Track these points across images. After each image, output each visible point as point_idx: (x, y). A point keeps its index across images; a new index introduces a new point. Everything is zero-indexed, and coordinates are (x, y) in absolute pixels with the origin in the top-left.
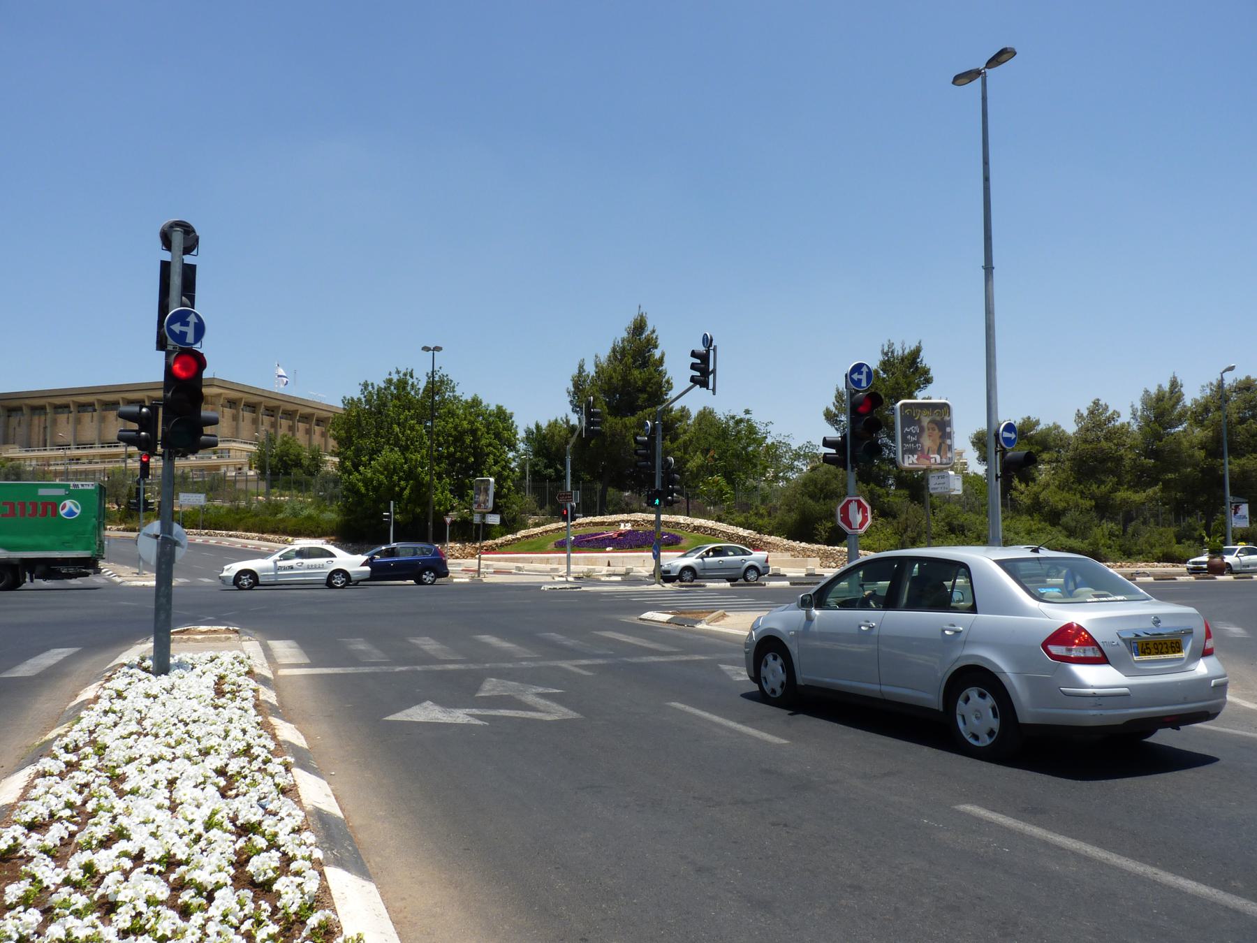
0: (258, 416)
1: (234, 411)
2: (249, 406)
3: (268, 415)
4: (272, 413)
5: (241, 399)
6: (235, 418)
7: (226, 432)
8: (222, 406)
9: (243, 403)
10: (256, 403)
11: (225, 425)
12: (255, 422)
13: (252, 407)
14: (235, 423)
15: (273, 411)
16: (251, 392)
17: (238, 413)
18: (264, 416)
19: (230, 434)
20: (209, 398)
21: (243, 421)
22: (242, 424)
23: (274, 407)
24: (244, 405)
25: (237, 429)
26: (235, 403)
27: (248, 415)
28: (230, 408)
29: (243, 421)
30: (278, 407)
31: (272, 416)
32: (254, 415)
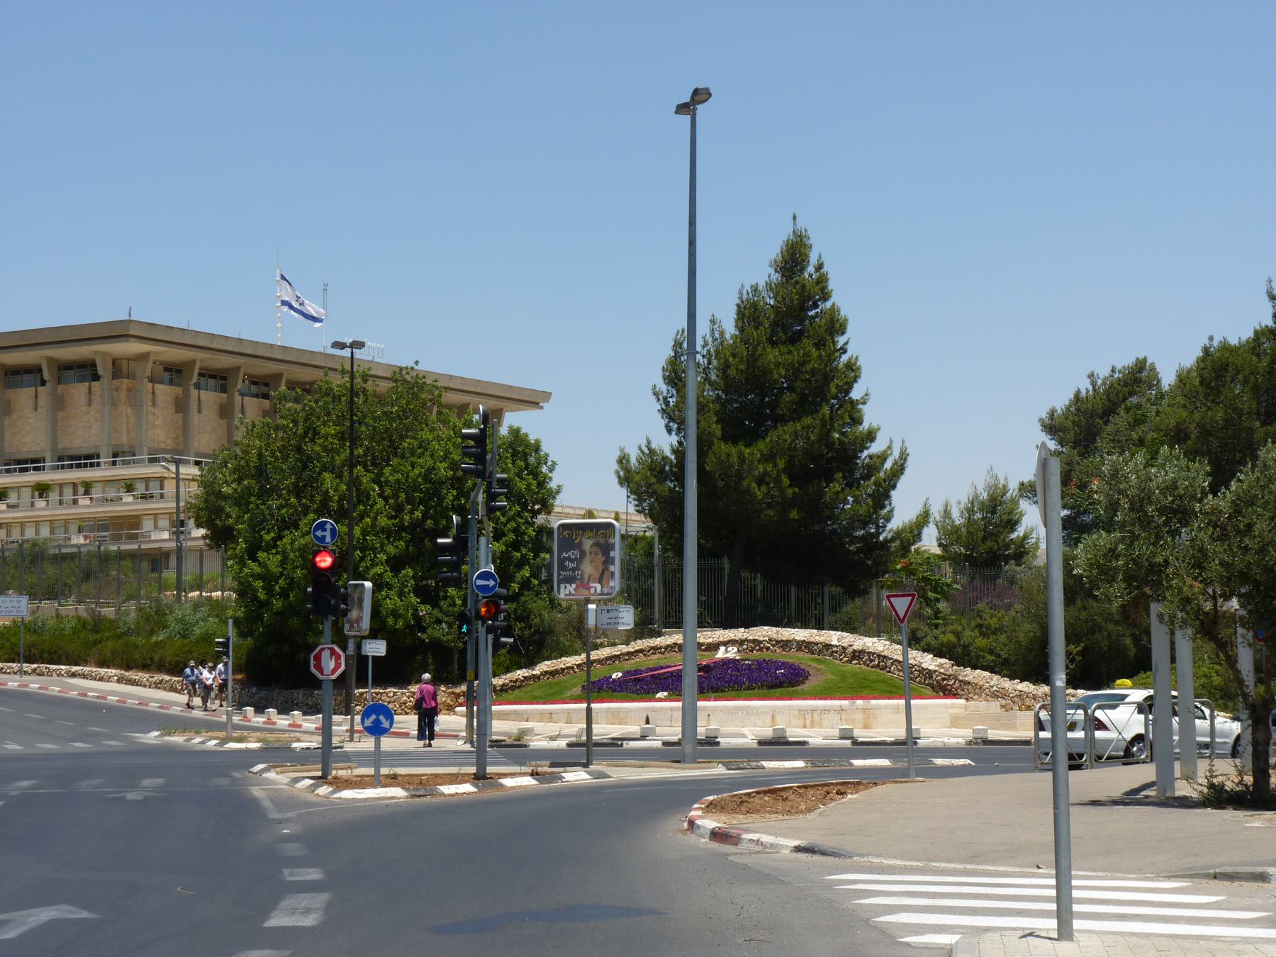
0: (231, 399)
1: (178, 390)
2: (213, 377)
3: (257, 396)
4: (264, 389)
5: (194, 361)
6: (181, 406)
7: (162, 438)
8: (152, 380)
9: (196, 371)
10: (227, 370)
11: (159, 422)
12: (225, 411)
13: (220, 379)
14: (181, 415)
15: (267, 385)
16: (214, 346)
17: (187, 394)
18: (247, 399)
19: (169, 442)
20: (125, 363)
21: (199, 411)
22: (195, 418)
23: (269, 376)
24: (200, 375)
25: (185, 427)
26: (179, 372)
27: (210, 397)
28: (171, 383)
29: (199, 411)
30: (277, 377)
31: (266, 396)
32: (225, 395)
